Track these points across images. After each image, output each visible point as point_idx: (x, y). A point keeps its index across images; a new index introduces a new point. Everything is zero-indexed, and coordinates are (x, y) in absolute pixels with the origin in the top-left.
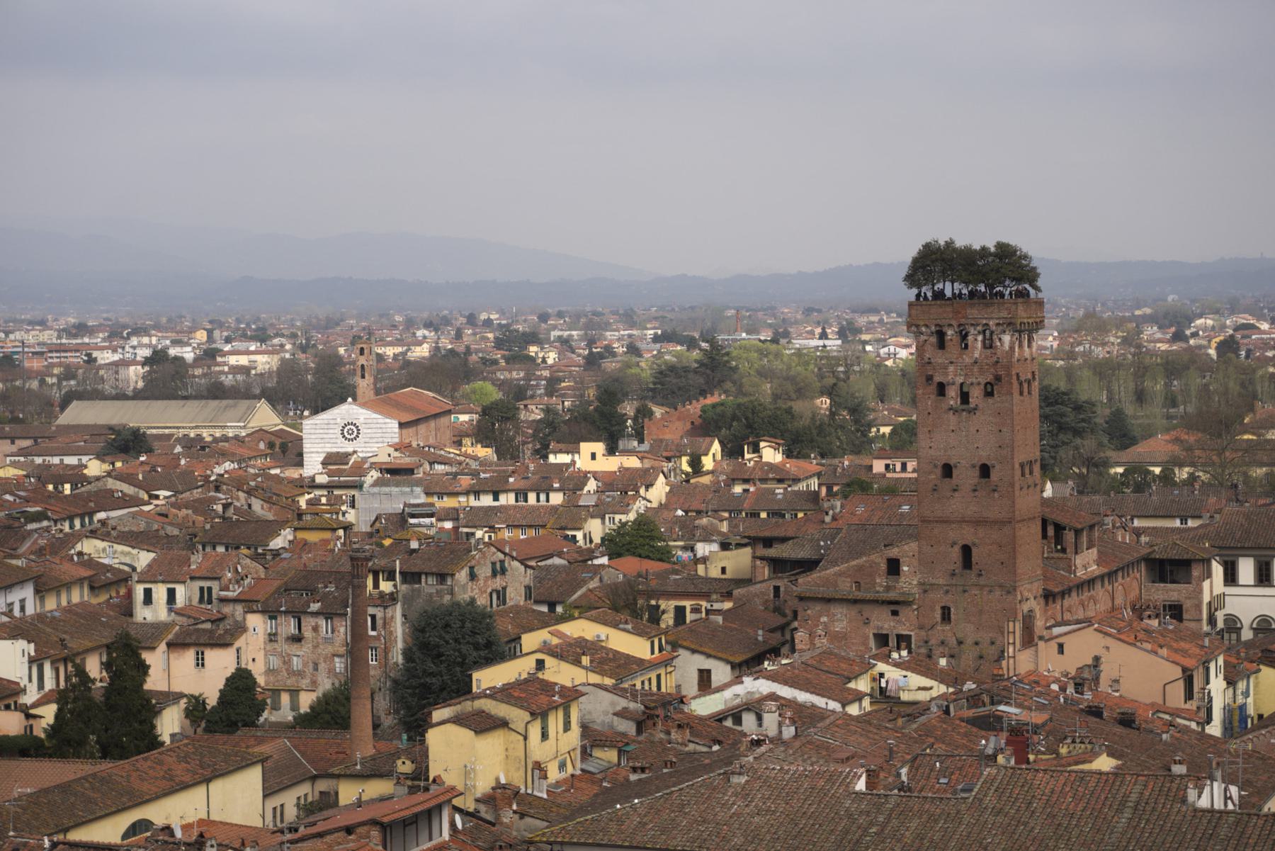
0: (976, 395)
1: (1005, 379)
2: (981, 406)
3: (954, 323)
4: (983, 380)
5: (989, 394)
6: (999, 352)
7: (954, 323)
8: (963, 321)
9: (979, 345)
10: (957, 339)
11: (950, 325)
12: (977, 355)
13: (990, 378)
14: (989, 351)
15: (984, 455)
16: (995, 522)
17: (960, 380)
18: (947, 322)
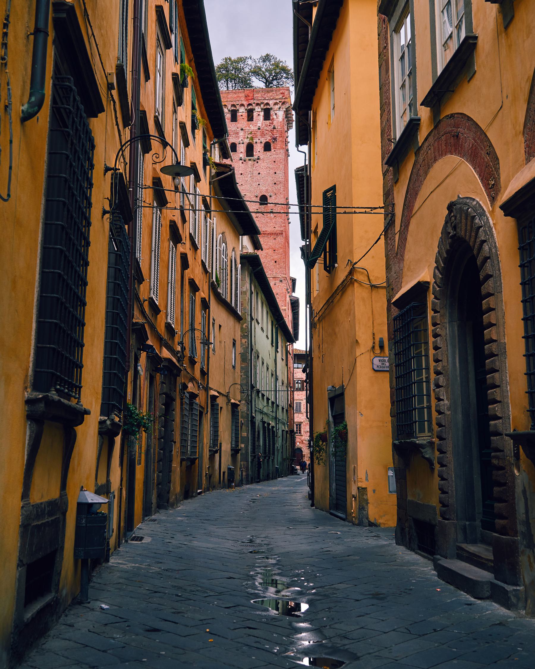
0: (258, 149)
1: (279, 139)
2: (261, 157)
3: (246, 103)
4: (264, 141)
5: (267, 147)
6: (275, 122)
7: (246, 103)
8: (251, 102)
9: (261, 118)
10: (245, 115)
11: (242, 105)
12: (259, 124)
13: (268, 138)
14: (268, 122)
15: (263, 190)
16: (271, 234)
17: (247, 141)
18: (240, 103)
